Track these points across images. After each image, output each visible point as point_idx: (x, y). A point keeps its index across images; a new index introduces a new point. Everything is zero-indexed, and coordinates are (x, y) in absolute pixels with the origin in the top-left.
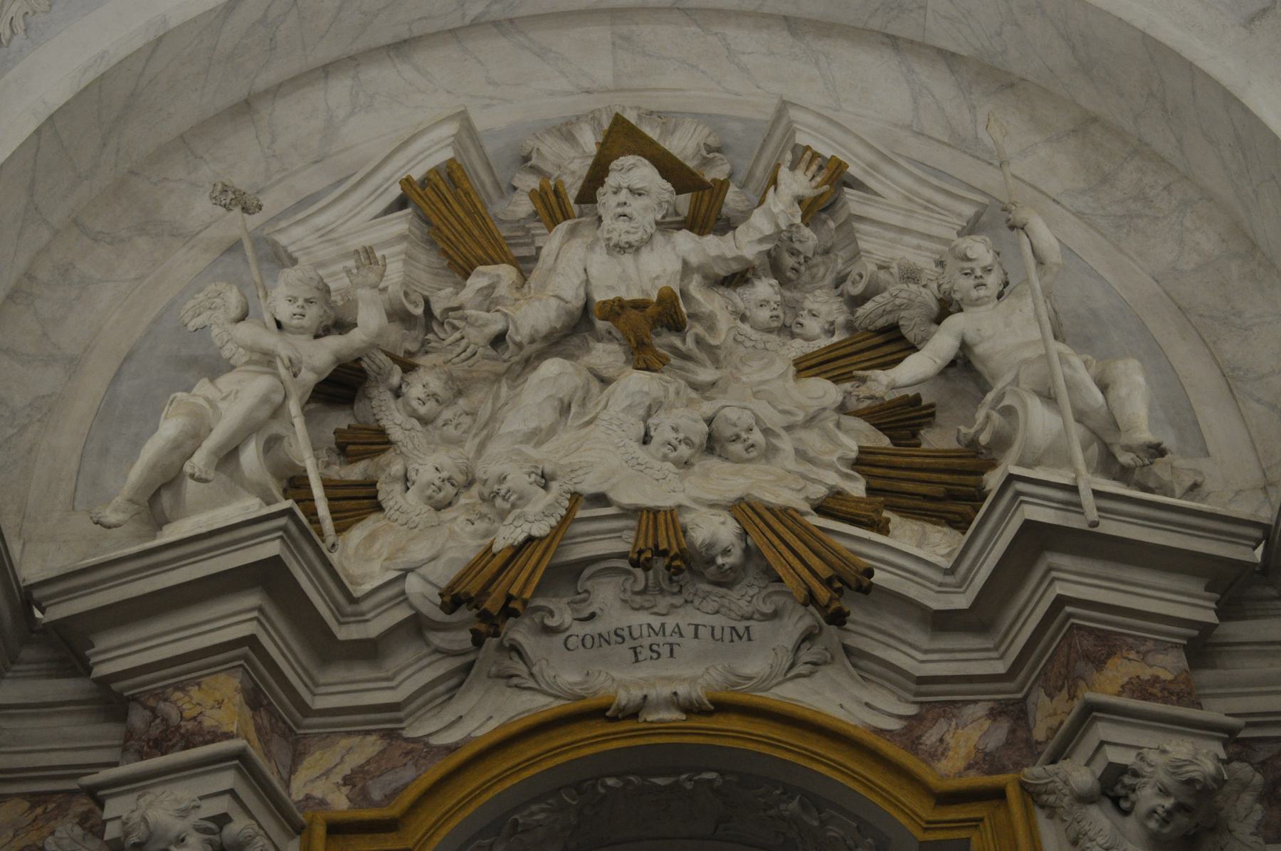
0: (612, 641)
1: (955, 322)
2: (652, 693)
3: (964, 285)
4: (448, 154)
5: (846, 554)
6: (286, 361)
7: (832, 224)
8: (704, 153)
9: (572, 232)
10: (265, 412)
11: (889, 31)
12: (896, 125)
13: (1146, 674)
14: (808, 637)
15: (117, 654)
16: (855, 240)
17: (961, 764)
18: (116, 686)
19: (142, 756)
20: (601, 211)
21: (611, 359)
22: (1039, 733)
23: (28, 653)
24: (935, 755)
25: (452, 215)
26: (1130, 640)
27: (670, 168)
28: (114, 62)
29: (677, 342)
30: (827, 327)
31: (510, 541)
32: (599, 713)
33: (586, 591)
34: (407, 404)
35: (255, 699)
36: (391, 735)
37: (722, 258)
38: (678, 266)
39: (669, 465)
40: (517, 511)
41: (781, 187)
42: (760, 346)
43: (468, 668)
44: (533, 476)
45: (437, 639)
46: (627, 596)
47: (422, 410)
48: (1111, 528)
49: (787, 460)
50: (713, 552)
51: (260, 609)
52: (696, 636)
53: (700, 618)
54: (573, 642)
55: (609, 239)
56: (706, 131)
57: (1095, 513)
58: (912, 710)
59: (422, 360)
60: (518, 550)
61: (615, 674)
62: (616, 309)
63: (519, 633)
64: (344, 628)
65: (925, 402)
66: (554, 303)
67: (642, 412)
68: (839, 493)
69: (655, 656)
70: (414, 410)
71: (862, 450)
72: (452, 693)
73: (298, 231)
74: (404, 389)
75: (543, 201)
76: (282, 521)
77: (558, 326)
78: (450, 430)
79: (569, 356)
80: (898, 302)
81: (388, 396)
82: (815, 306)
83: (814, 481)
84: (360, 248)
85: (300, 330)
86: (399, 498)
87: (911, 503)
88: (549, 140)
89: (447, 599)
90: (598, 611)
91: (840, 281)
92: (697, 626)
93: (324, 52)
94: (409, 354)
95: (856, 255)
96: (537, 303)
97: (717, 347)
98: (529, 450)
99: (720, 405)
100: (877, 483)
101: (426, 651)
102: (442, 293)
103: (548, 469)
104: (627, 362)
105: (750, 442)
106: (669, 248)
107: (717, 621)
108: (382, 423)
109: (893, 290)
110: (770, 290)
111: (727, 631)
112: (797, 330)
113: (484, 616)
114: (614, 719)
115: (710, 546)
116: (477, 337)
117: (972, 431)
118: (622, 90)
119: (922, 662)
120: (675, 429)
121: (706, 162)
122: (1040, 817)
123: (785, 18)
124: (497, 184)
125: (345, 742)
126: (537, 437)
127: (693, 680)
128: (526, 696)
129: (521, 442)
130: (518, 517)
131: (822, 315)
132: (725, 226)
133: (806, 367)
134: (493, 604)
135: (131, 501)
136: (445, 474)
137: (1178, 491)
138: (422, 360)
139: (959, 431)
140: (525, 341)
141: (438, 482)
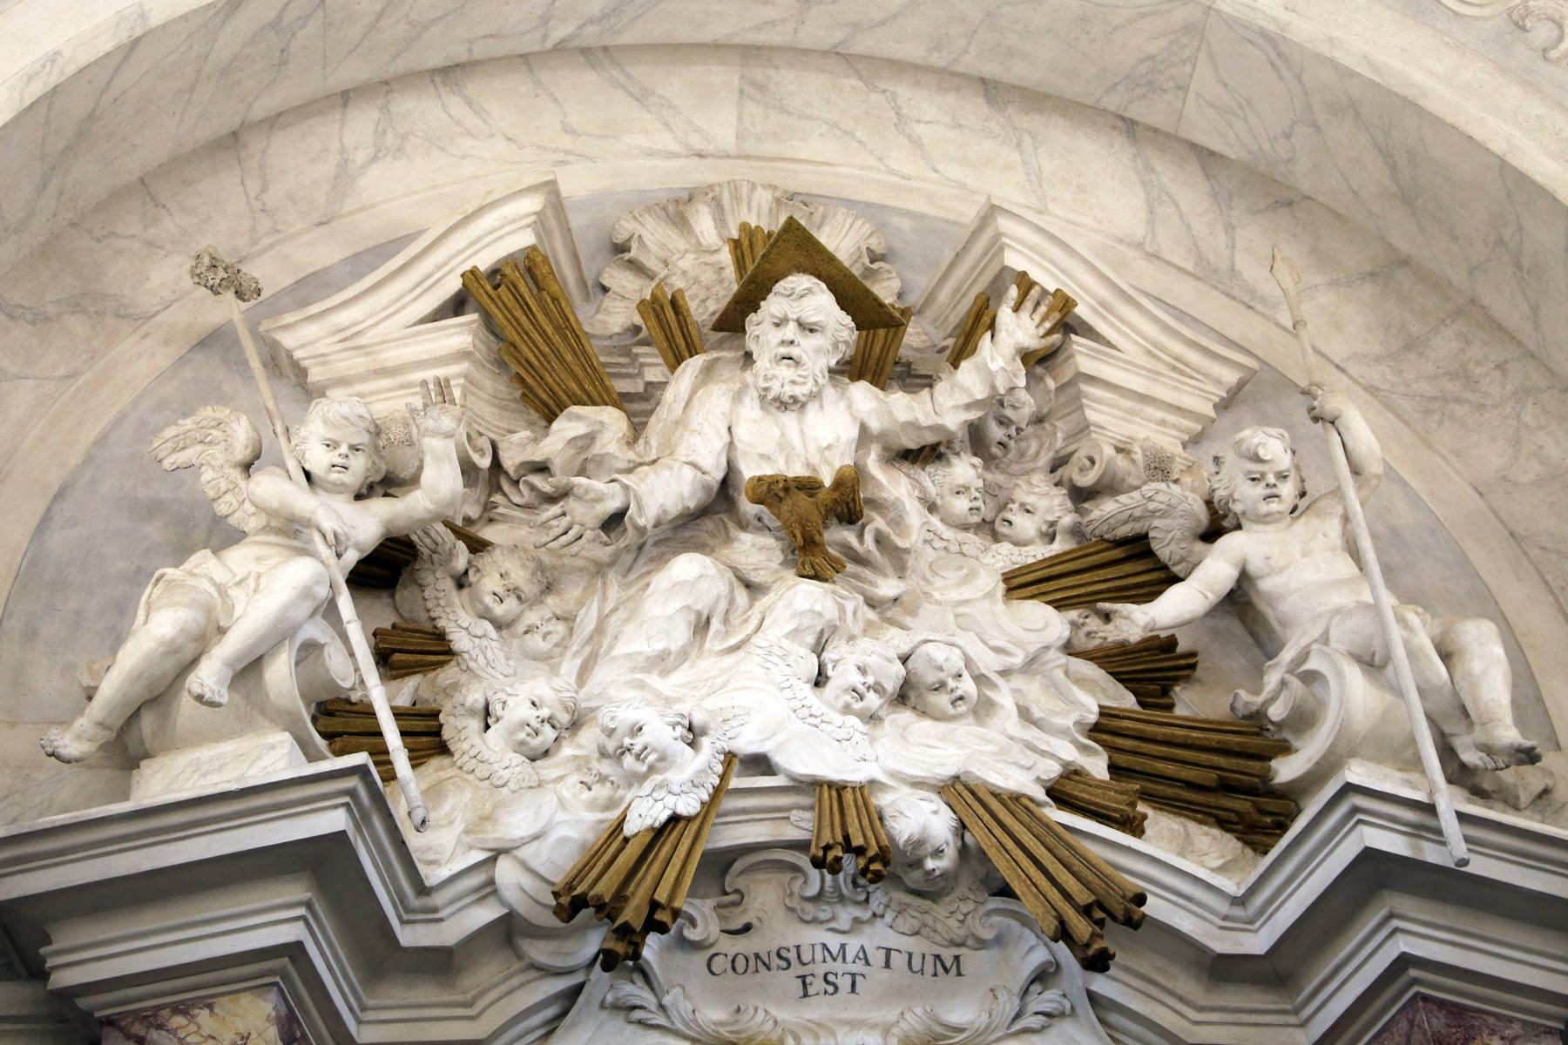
0: (773, 965)
1: (1229, 542)
3: (1246, 495)
4: (526, 239)
5: (1109, 870)
6: (330, 537)
7: (1051, 384)
9: (708, 371)
11: (1126, 114)
12: (1121, 241)
14: (1044, 976)
16: (1081, 407)
18: (84, 1003)
20: (751, 345)
21: (763, 557)
26: (1491, 1020)
27: (851, 295)
28: (71, 69)
29: (854, 541)
30: (1044, 528)
31: (648, 822)
33: (737, 891)
34: (476, 599)
37: (913, 426)
38: (854, 433)
39: (853, 720)
40: (657, 778)
41: (1002, 335)
42: (954, 548)
43: (577, 990)
44: (679, 728)
45: (538, 951)
46: (795, 903)
47: (499, 610)
48: (1481, 866)
49: (1007, 719)
50: (920, 852)
51: (308, 905)
52: (887, 965)
53: (894, 940)
54: (720, 964)
55: (766, 389)
57: (1464, 846)
60: (659, 833)
61: (776, 1012)
62: (774, 492)
64: (408, 928)
66: (688, 473)
68: (1076, 772)
69: (831, 989)
70: (488, 609)
71: (1104, 712)
73: (310, 331)
74: (472, 577)
75: (657, 316)
76: (353, 782)
77: (692, 505)
78: (536, 642)
79: (700, 547)
80: (1152, 506)
81: (449, 584)
82: (1030, 499)
83: (1043, 753)
84: (396, 365)
85: (338, 488)
86: (476, 740)
87: (1170, 791)
88: (649, 221)
89: (565, 900)
90: (755, 922)
91: (1058, 464)
92: (889, 951)
93: (351, 73)
94: (468, 521)
95: (1084, 429)
96: (666, 473)
97: (907, 551)
98: (654, 680)
99: (920, 638)
100: (1123, 760)
101: (517, 965)
102: (516, 437)
103: (698, 719)
104: (786, 563)
105: (959, 693)
106: (842, 405)
108: (441, 623)
110: (972, 472)
111: (930, 960)
112: (1003, 529)
115: (919, 843)
117: (1260, 699)
118: (748, 157)
119: (1196, 1023)
120: (862, 670)
123: (983, 81)
124: (582, 282)
126: (662, 662)
129: (643, 670)
130: (660, 786)
131: (1040, 515)
132: (913, 378)
133: (1019, 584)
134: (632, 913)
135: (101, 725)
136: (545, 713)
137: (1524, 799)
139: (1236, 696)
140: (649, 526)
141: (534, 723)
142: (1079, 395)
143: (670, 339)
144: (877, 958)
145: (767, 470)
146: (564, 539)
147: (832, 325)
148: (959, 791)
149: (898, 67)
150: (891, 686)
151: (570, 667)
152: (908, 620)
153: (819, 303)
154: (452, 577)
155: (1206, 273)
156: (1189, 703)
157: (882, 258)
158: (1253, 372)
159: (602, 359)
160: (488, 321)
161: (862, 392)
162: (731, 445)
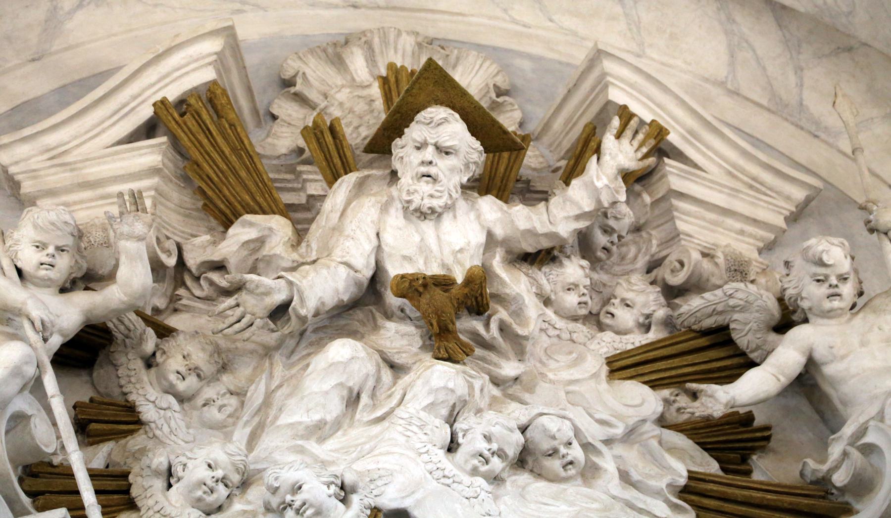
1: (798, 333)
3: (813, 294)
4: (208, 75)
6: (38, 324)
8: (494, 96)
9: (360, 187)
12: (707, 80)
16: (672, 219)
20: (396, 165)
21: (405, 342)
25: (213, 150)
27: (480, 123)
30: (641, 320)
34: (162, 377)
37: (531, 233)
38: (482, 238)
39: (480, 481)
41: (606, 158)
42: (565, 336)
44: (333, 487)
47: (181, 386)
55: (409, 202)
56: (494, 68)
62: (415, 287)
65: (757, 423)
66: (343, 271)
67: (445, 412)
70: (172, 386)
71: (692, 476)
73: (24, 150)
74: (159, 358)
75: (318, 140)
77: (346, 298)
78: (213, 414)
79: (353, 334)
80: (732, 302)
81: (139, 364)
82: (630, 295)
85: (45, 283)
86: (160, 497)
88: (312, 61)
91: (653, 265)
94: (157, 311)
95: (675, 237)
96: (324, 272)
97: (526, 338)
98: (312, 446)
99: (536, 411)
103: (349, 479)
104: (424, 347)
105: (569, 458)
106: (472, 215)
108: (131, 398)
110: (580, 272)
112: (607, 321)
116: (255, 305)
117: (825, 468)
120: (488, 438)
124: (255, 111)
126: (320, 431)
129: (302, 437)
132: (532, 193)
133: (621, 367)
136: (219, 473)
139: (805, 464)
140: (310, 316)
141: (210, 483)
142: (670, 209)
143: (328, 160)
145: (409, 269)
146: (237, 326)
147: (464, 149)
150: (512, 452)
151: (241, 434)
152: (526, 396)
153: (453, 130)
154: (142, 358)
155: (778, 107)
156: (765, 469)
157: (506, 93)
158: (818, 191)
159: (271, 175)
160: (175, 143)
161: (489, 205)
162: (379, 248)
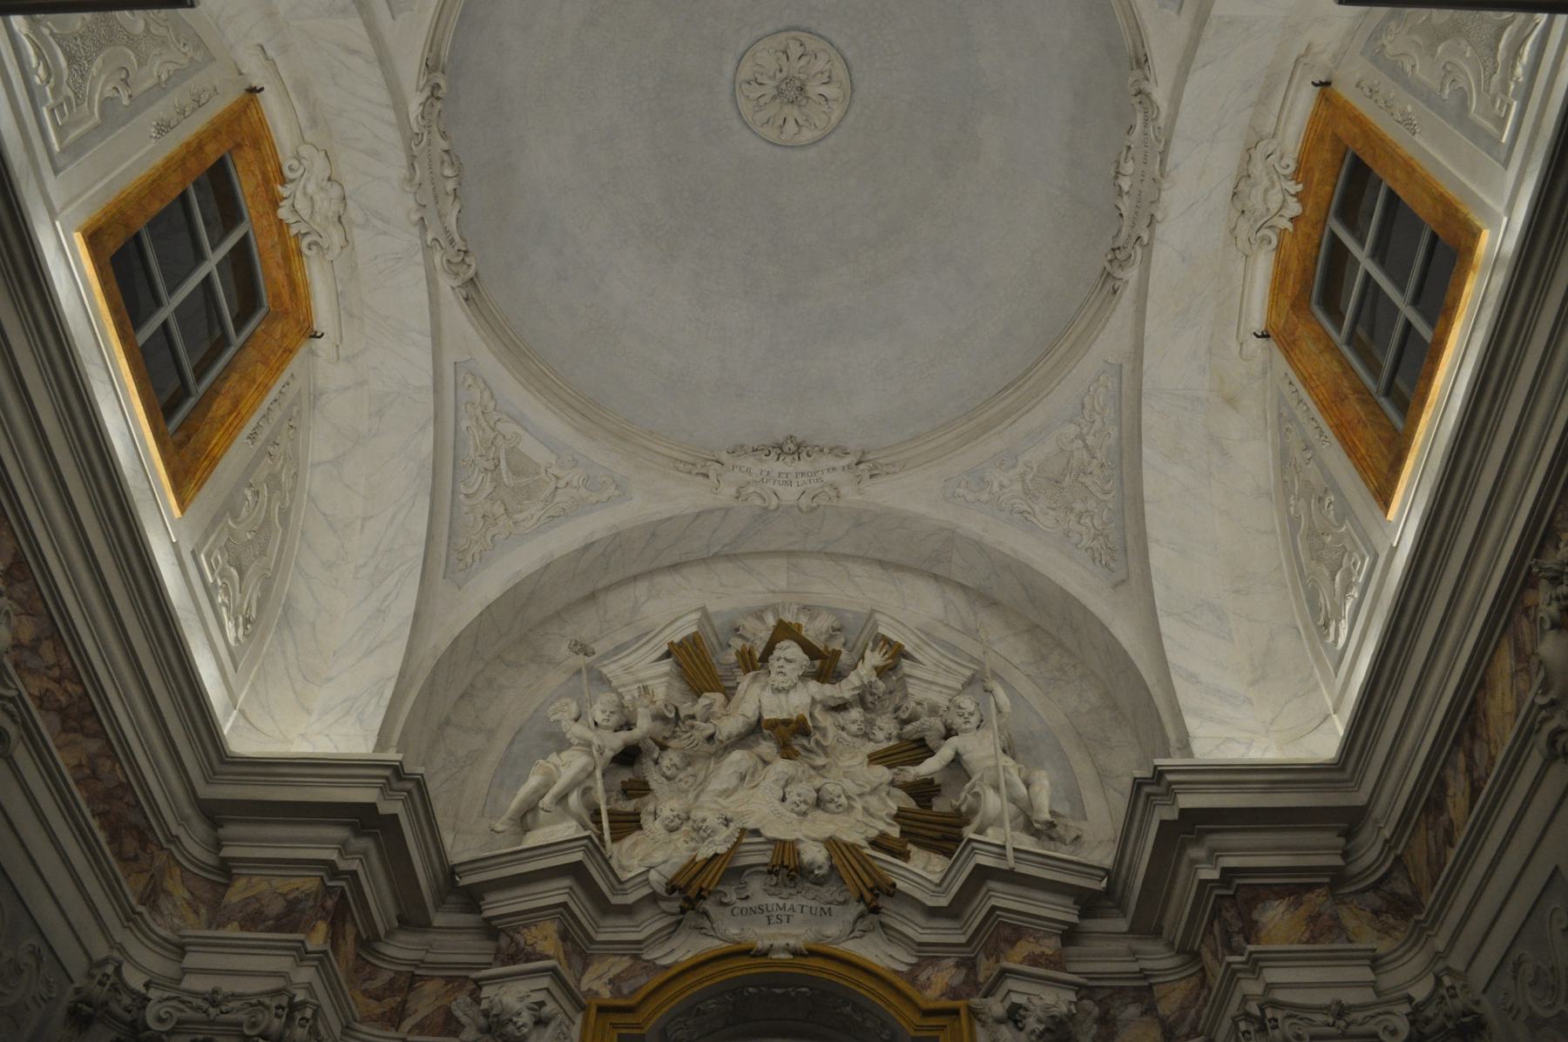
1: (953, 740)
2: (776, 943)
3: (958, 722)
4: (694, 629)
9: (755, 678)
10: (584, 775)
13: (1038, 950)
14: (861, 916)
15: (498, 905)
17: (938, 993)
19: (504, 964)
22: (981, 978)
23: (452, 898)
24: (925, 987)
25: (695, 664)
27: (808, 648)
29: (805, 742)
32: (747, 953)
35: (564, 936)
36: (636, 957)
38: (809, 700)
43: (679, 922)
45: (664, 905)
48: (1023, 869)
49: (859, 813)
58: (913, 960)
59: (672, 743)
62: (774, 725)
63: (708, 906)
71: (899, 809)
72: (669, 936)
73: (613, 666)
81: (651, 763)
84: (646, 676)
85: (607, 728)
91: (897, 709)
94: (665, 738)
95: (906, 696)
98: (721, 800)
107: (812, 903)
109: (924, 719)
113: (687, 899)
114: (754, 956)
115: (811, 864)
116: (699, 735)
121: (831, 637)
122: (978, 1028)
125: (611, 959)
126: (726, 793)
127: (797, 936)
128: (709, 940)
131: (886, 727)
133: (874, 759)
134: (692, 893)
138: (672, 743)
144: (798, 909)
145: (773, 716)
148: (831, 843)
149: (847, 557)
151: (691, 796)
156: (941, 805)
161: (814, 687)
